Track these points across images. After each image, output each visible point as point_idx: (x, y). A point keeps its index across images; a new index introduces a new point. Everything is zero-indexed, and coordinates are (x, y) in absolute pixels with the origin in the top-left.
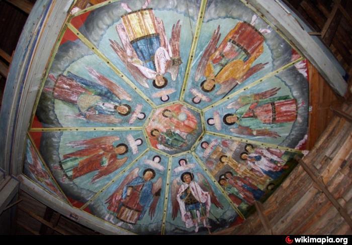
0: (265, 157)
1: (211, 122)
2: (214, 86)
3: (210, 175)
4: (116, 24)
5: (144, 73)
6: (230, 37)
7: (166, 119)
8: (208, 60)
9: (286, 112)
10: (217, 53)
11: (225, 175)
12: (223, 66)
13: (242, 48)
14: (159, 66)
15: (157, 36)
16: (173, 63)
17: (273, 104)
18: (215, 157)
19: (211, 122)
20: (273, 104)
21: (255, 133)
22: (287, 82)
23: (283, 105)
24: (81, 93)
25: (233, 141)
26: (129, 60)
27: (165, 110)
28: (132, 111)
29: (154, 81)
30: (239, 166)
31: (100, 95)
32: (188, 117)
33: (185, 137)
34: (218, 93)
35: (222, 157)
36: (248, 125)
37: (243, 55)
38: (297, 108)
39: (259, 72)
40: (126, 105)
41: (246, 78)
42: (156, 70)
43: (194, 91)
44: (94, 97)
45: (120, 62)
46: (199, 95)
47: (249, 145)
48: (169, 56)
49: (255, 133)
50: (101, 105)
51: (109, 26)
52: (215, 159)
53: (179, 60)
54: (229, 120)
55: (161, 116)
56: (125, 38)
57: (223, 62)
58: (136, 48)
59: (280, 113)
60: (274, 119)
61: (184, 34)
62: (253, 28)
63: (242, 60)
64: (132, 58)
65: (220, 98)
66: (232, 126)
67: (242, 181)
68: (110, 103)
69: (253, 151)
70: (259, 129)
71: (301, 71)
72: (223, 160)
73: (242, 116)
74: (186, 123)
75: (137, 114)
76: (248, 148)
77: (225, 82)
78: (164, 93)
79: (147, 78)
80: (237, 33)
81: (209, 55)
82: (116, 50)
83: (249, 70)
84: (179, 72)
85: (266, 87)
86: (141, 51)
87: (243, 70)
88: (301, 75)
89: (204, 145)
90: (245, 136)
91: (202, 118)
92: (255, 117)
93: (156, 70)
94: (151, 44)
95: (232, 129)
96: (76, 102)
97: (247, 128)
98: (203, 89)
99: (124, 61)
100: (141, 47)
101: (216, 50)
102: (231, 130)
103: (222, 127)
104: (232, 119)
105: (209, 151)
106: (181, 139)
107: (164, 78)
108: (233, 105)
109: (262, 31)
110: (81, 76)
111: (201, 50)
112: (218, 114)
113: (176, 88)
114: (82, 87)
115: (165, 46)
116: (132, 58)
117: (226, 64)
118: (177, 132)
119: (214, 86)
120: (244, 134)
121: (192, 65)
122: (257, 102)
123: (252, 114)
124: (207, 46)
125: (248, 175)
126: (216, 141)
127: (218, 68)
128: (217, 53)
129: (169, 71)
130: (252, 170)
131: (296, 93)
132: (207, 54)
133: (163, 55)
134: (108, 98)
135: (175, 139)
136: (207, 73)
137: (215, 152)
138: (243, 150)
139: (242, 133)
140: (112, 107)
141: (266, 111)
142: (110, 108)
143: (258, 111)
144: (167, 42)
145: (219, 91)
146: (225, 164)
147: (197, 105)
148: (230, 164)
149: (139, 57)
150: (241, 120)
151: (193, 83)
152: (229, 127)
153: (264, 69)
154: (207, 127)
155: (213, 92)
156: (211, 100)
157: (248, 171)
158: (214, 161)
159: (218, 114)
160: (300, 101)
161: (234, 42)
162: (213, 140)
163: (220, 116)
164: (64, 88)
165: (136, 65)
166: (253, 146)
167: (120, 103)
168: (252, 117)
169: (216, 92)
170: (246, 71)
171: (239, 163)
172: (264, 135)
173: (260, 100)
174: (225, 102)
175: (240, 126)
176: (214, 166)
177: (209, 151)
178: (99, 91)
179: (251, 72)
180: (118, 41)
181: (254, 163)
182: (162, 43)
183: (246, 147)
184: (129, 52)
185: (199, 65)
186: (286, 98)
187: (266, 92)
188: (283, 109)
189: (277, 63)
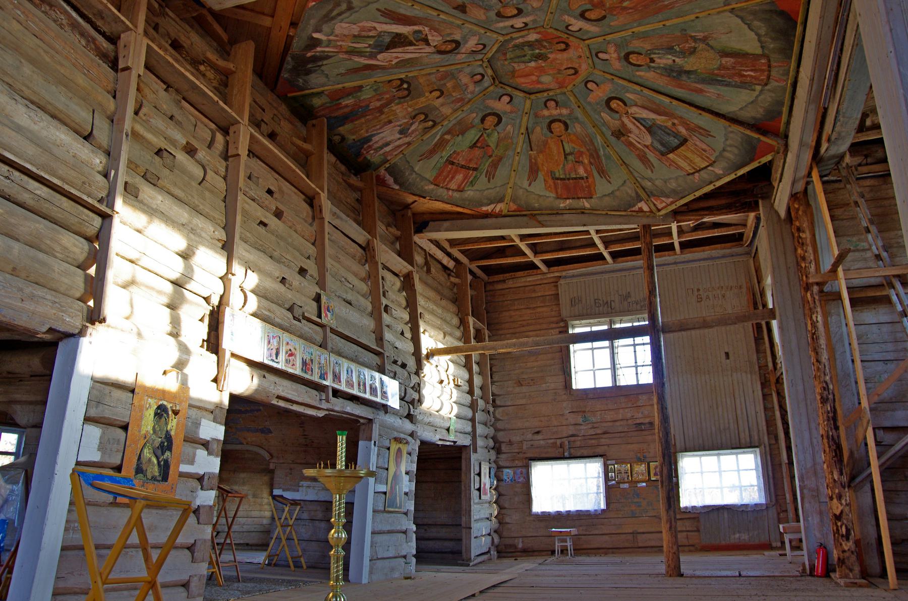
0: (399, 139)
1: (506, 99)
2: (552, 132)
3: (423, 72)
4: (717, 154)
5: (646, 111)
6: (590, 180)
7: (565, 67)
8: (588, 150)
9: (453, 178)
10: (586, 161)
11: (407, 89)
12: (566, 155)
13: (569, 179)
14: (634, 124)
15: (663, 154)
16: (620, 133)
17: (475, 169)
18: (449, 85)
19: (506, 99)
20: (475, 169)
21: (447, 137)
22: (490, 191)
23: (465, 178)
24: (719, 69)
25: (455, 111)
26: (676, 121)
27: (576, 72)
28: (623, 60)
29: (625, 104)
30: (409, 109)
31: (688, 73)
32: (539, 82)
33: (515, 65)
34: (538, 129)
35: (442, 93)
36: (466, 135)
37: (559, 173)
38: (448, 189)
39: (527, 174)
40: (639, 66)
41: (530, 161)
42: (634, 118)
43: (565, 111)
44: (695, 68)
45: (685, 116)
46: (553, 111)
47: (433, 126)
48: (633, 138)
49: (447, 137)
50: (677, 60)
51: (724, 150)
52: (445, 84)
53: (618, 138)
54: (491, 120)
55: (576, 66)
56: (695, 141)
57: (570, 157)
58: (676, 135)
59: (456, 172)
60: (453, 163)
61: (636, 164)
62: (578, 198)
63: (556, 171)
64: (674, 124)
65: (530, 126)
66: (479, 118)
67: (377, 108)
68: (666, 64)
69: (421, 127)
70: (451, 143)
71: (492, 206)
72: (437, 94)
73: (485, 135)
74: (534, 78)
75: (612, 55)
76: (431, 123)
77: (546, 143)
78: (599, 94)
79: (636, 105)
80: (589, 187)
81: (591, 155)
82: (701, 128)
83: (538, 168)
84: (605, 124)
85: (502, 172)
86: (669, 134)
87: (543, 165)
88: (489, 205)
89: (479, 77)
90: (450, 125)
91: (522, 94)
92: (474, 146)
93: (634, 118)
94: (662, 144)
95: (475, 118)
96: (722, 57)
97: (463, 133)
98: (560, 121)
99: (681, 118)
100: (672, 138)
101: (591, 163)
102: (474, 115)
103: (487, 107)
104: (489, 123)
105: (465, 79)
106: (517, 60)
107: (617, 112)
108: (509, 132)
109: (568, 201)
110: (732, 89)
111: (605, 155)
112: (511, 112)
113: (589, 103)
114: (722, 76)
115: (647, 147)
116: (674, 124)
117: (565, 158)
118: (533, 64)
119: (552, 132)
120: (454, 125)
121: (599, 137)
122: (490, 156)
123: (479, 145)
124: (604, 161)
125: (383, 116)
126: (472, 93)
127: (568, 150)
128: (586, 161)
129: (617, 123)
130: (390, 122)
131: (470, 193)
132: (595, 156)
133: (641, 137)
134: (672, 71)
135: (525, 56)
136: (574, 138)
137: (457, 87)
138: (431, 117)
139: (459, 123)
140: (657, 60)
141: (471, 160)
142: (659, 58)
143: (477, 152)
144: (646, 150)
145: (539, 132)
146: (427, 94)
147: (544, 100)
148: (423, 99)
149: (666, 127)
150: (480, 131)
151: (577, 118)
152: (481, 115)
153: (526, 178)
154: (501, 91)
155: (545, 126)
156: (536, 116)
157: (392, 118)
158: (442, 82)
159: (511, 112)
160: (456, 195)
161: (582, 178)
162: (477, 89)
163: (505, 113)
164: (752, 70)
165: (663, 118)
166: (427, 130)
167: (649, 67)
168: (475, 143)
169: (542, 129)
170: (540, 166)
171: (415, 110)
172: (436, 145)
173: (490, 160)
174: (520, 127)
175: (473, 126)
176: (434, 80)
177: (465, 79)
178: (692, 76)
179: (534, 171)
180: (702, 138)
181: (400, 126)
182: (651, 148)
183: (433, 121)
184: (683, 130)
185: (591, 141)
186: (472, 184)
187: (496, 168)
188: (459, 177)
189: (521, 192)
